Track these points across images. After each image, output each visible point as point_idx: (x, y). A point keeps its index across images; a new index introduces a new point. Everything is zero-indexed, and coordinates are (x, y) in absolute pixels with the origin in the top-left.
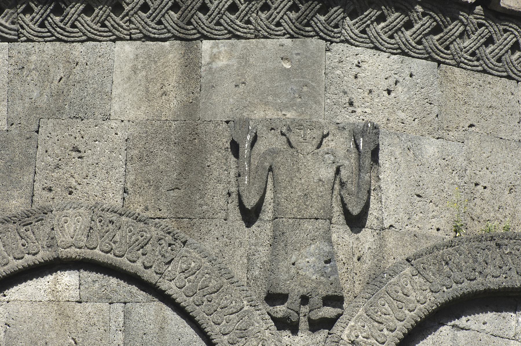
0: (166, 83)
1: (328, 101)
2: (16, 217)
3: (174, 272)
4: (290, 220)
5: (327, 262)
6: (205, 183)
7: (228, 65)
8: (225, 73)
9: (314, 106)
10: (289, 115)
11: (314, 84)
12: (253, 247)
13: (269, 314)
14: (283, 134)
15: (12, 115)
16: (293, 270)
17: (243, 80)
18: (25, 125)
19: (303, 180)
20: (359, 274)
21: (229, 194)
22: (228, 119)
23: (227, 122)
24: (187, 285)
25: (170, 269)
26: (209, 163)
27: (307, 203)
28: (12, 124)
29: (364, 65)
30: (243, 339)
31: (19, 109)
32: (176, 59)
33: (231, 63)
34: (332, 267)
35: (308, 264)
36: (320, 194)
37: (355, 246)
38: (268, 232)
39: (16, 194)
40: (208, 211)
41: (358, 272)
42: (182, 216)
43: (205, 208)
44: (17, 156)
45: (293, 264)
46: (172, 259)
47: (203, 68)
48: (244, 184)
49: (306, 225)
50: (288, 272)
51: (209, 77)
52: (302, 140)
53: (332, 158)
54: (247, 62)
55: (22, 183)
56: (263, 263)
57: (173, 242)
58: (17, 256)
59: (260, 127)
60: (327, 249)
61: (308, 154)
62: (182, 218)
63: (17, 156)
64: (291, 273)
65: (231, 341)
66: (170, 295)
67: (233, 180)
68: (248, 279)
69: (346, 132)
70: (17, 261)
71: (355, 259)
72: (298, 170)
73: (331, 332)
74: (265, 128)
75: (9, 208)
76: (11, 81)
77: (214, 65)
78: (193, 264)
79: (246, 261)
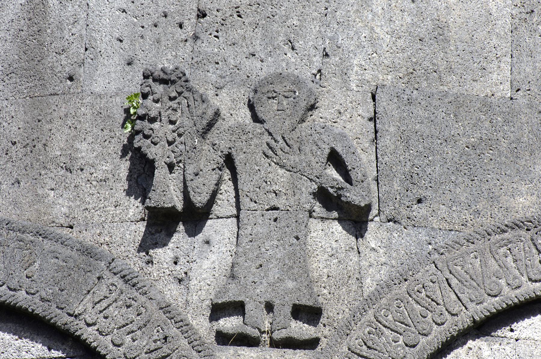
2: (531, 222)
15: (517, 77)
18: (536, 93)
28: (518, 90)
31: (528, 70)
39: (524, 189)
44: (525, 136)
55: (533, 175)
58: (533, 277)
63: (525, 136)
70: (534, 283)
75: (514, 207)
76: (516, 28)
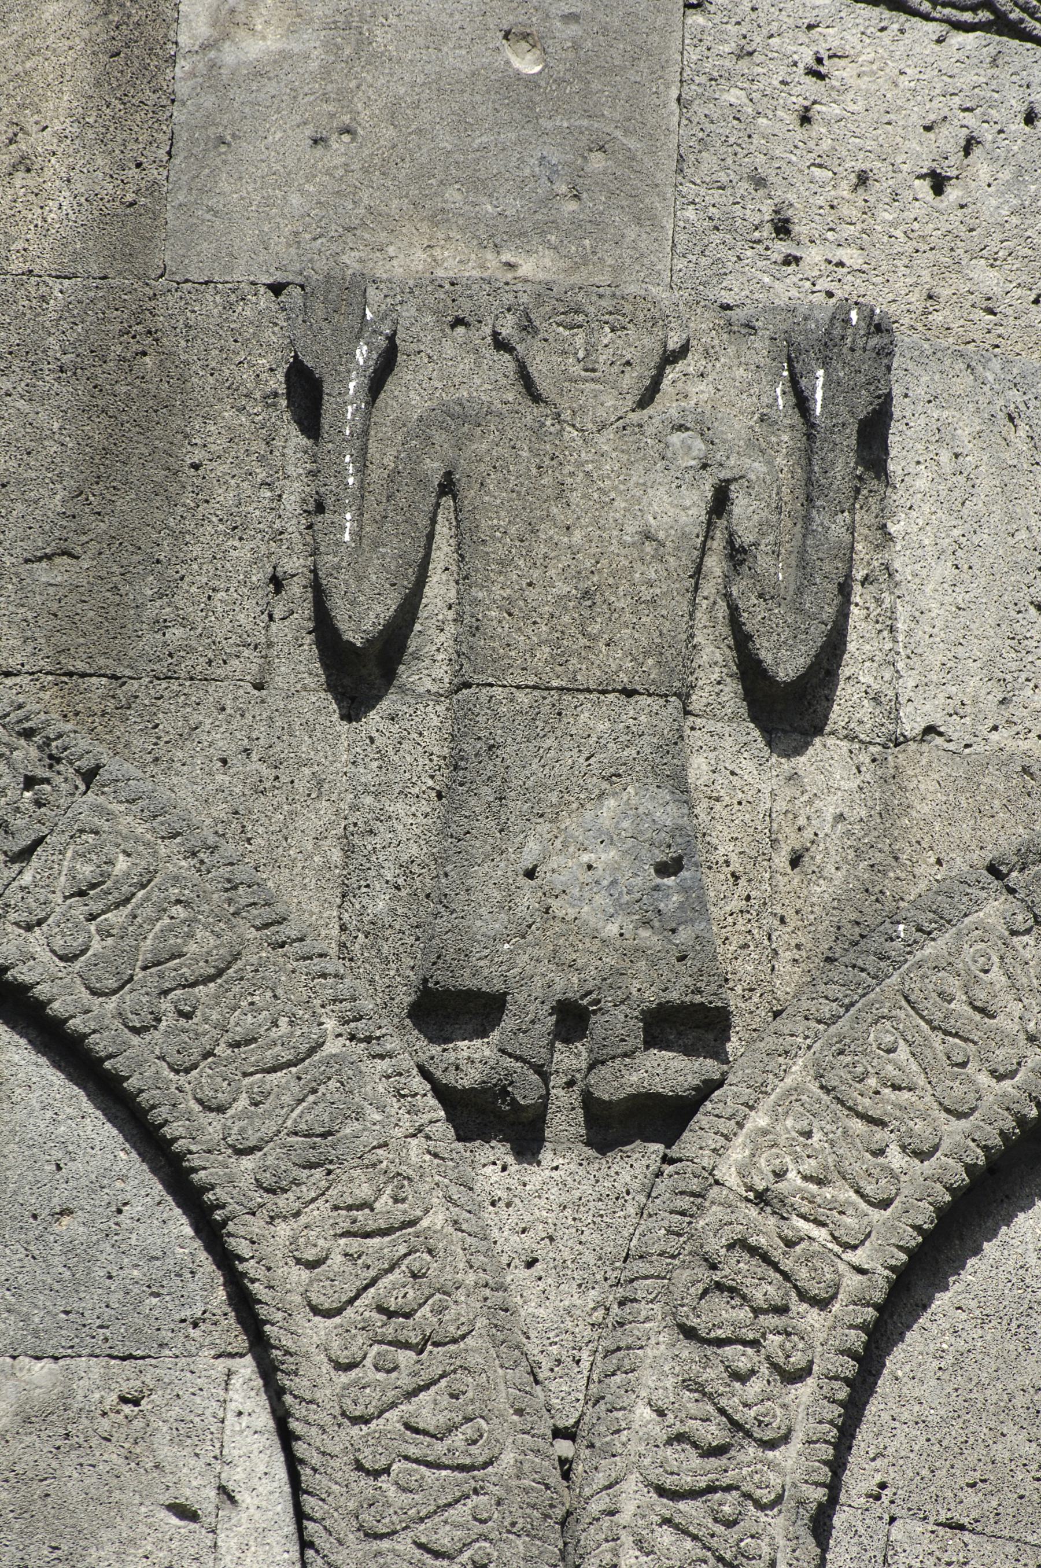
0: (30, 120)
1: (690, 213)
3: (42, 894)
4: (520, 695)
5: (668, 868)
6: (178, 536)
7: (284, 56)
8: (272, 88)
9: (631, 233)
10: (527, 268)
11: (632, 143)
12: (368, 800)
13: (425, 1074)
14: (501, 344)
16: (527, 898)
17: (346, 119)
19: (577, 536)
20: (793, 921)
21: (277, 583)
22: (279, 277)
23: (277, 289)
24: (96, 945)
25: (27, 878)
26: (198, 456)
27: (593, 629)
29: (840, 72)
30: (318, 1173)
32: (72, 24)
33: (296, 47)
34: (685, 890)
35: (588, 877)
36: (646, 594)
37: (780, 805)
38: (430, 739)
40: (190, 650)
41: (789, 913)
42: (81, 666)
43: (177, 634)
45: (530, 874)
46: (39, 841)
47: (184, 65)
48: (338, 543)
49: (584, 717)
50: (507, 905)
51: (209, 101)
52: (577, 370)
53: (699, 446)
54: (363, 43)
56: (406, 868)
57: (41, 772)
59: (408, 312)
60: (668, 815)
61: (602, 428)
62: (83, 675)
64: (521, 911)
65: (268, 1179)
66: (28, 988)
67: (294, 527)
68: (343, 928)
69: (760, 343)
71: (781, 860)
72: (561, 491)
73: (674, 1152)
74: (429, 319)
77: (229, 56)
78: (122, 864)
79: (336, 856)
